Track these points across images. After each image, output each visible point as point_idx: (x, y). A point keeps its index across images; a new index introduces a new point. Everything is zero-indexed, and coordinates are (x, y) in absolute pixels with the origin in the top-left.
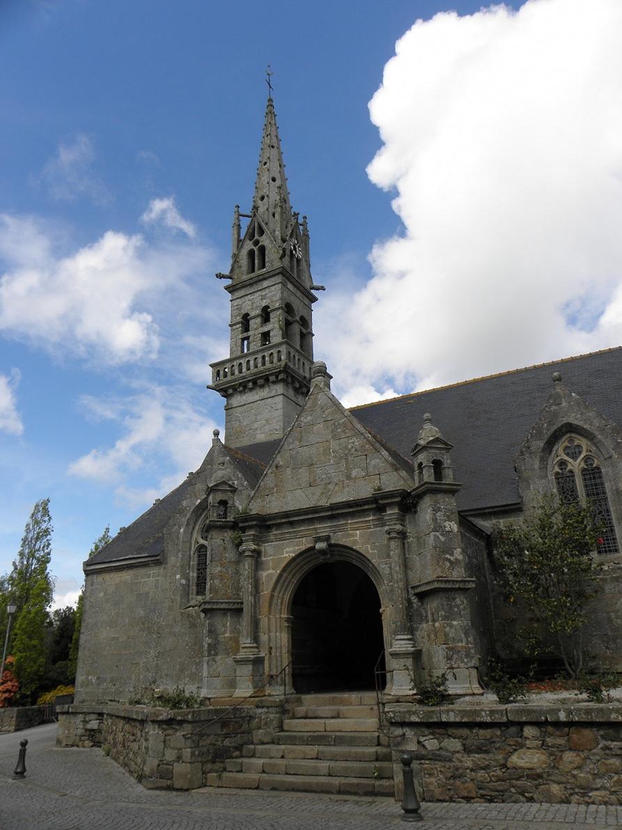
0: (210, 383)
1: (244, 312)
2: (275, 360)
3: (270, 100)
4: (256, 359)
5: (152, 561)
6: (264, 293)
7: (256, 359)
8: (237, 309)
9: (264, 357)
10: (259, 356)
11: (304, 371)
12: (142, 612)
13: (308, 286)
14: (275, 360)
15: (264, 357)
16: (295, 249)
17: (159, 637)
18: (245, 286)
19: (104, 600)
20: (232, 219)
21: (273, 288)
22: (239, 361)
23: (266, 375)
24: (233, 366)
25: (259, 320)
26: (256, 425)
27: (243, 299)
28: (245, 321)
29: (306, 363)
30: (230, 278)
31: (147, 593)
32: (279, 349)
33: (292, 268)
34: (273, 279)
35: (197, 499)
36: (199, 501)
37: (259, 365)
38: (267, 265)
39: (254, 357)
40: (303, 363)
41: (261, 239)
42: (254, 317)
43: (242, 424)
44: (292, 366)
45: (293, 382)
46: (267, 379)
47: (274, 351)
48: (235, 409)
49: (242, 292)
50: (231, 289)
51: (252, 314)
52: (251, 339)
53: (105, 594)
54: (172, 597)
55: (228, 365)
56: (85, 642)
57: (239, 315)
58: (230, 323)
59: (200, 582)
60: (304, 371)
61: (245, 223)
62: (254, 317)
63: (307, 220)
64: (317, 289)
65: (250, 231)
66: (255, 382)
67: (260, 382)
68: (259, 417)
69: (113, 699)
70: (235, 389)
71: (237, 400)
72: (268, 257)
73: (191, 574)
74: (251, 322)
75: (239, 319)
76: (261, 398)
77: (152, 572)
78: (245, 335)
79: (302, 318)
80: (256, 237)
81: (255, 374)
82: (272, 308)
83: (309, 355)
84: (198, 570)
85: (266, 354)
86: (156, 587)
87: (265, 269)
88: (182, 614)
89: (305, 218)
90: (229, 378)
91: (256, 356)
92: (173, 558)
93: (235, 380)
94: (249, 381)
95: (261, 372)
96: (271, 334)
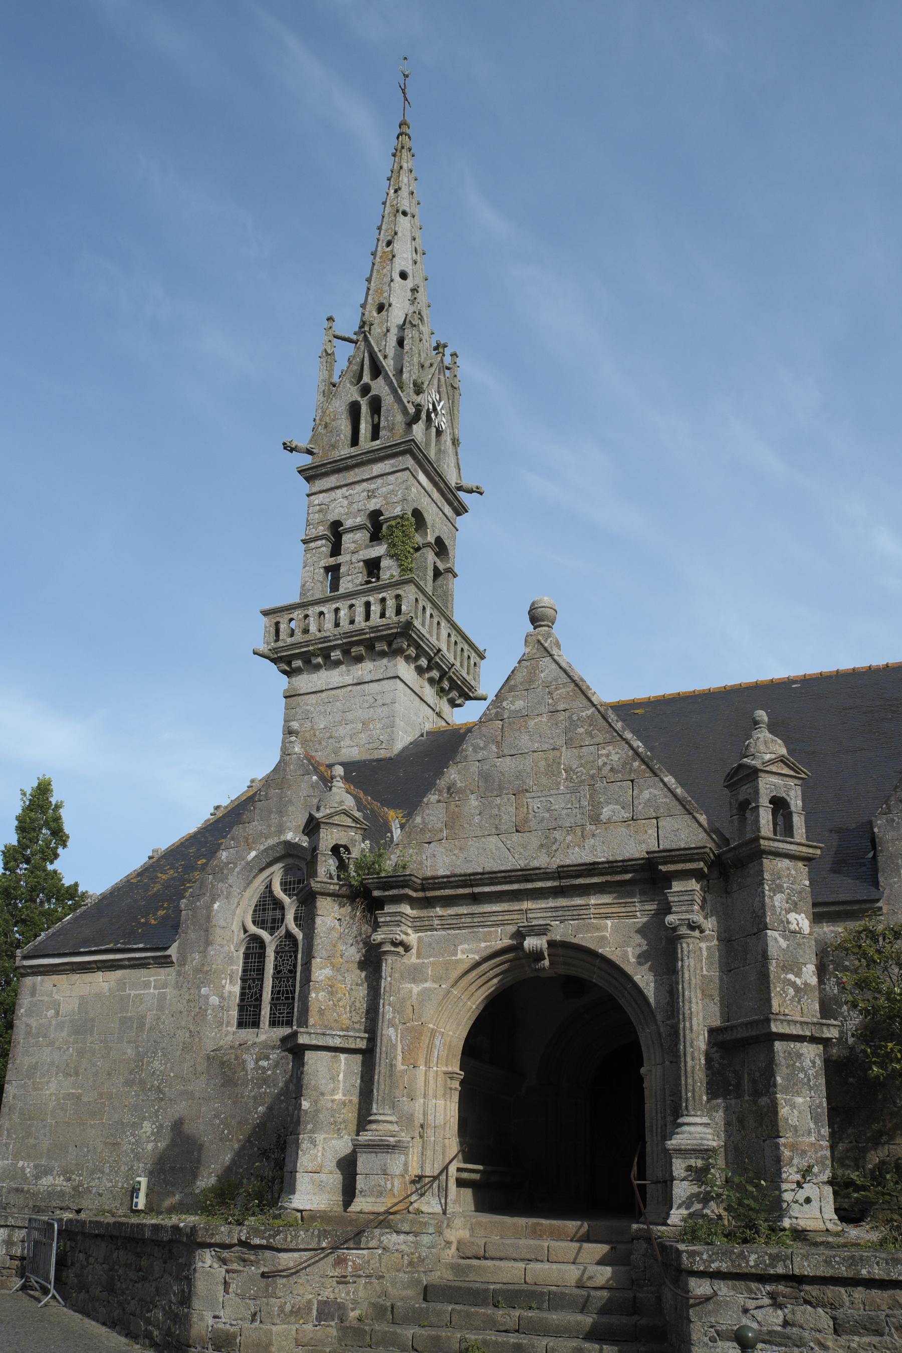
0: (263, 648)
1: (332, 517)
2: (390, 612)
3: (402, 124)
4: (351, 606)
5: (153, 957)
6: (373, 486)
7: (351, 606)
8: (320, 511)
9: (368, 605)
10: (359, 603)
11: (438, 639)
12: (129, 1051)
13: (453, 481)
14: (390, 612)
15: (368, 605)
16: (435, 409)
17: (162, 1099)
18: (338, 471)
19: (54, 1022)
20: (319, 340)
21: (391, 478)
22: (318, 609)
23: (370, 638)
24: (306, 616)
25: (362, 536)
26: (341, 731)
27: (333, 494)
28: (336, 530)
29: (443, 624)
30: (309, 452)
31: (142, 1018)
32: (353, 602)
33: (428, 443)
34: (392, 461)
35: (251, 849)
36: (253, 854)
37: (357, 619)
38: (382, 433)
39: (334, 606)
40: (439, 623)
41: (373, 384)
42: (352, 530)
43: (316, 727)
44: (419, 627)
45: (417, 658)
46: (325, 653)
47: (389, 595)
48: (302, 697)
49: (331, 481)
50: (310, 474)
51: (348, 523)
52: (343, 569)
53: (57, 1013)
54: (192, 1028)
55: (298, 614)
56: (14, 1098)
57: (320, 522)
58: (304, 537)
59: (245, 1003)
60: (438, 639)
61: (343, 352)
62: (352, 530)
63: (458, 360)
64: (470, 491)
65: (355, 368)
66: (325, 653)
67: (336, 655)
68: (349, 716)
69: (64, 1205)
70: (307, 658)
71: (306, 682)
72: (386, 418)
73: (228, 988)
74: (346, 539)
75: (322, 530)
76: (355, 681)
77: (152, 979)
78: (332, 561)
79: (439, 541)
80: (366, 379)
81: (347, 635)
82: (348, 523)
83: (447, 607)
84: (243, 980)
85: (371, 599)
86: (161, 1008)
87: (378, 442)
88: (209, 1058)
89: (454, 355)
90: (299, 637)
91: (353, 602)
92: (197, 956)
93: (307, 643)
94: (334, 648)
95: (361, 632)
96: (382, 564)
